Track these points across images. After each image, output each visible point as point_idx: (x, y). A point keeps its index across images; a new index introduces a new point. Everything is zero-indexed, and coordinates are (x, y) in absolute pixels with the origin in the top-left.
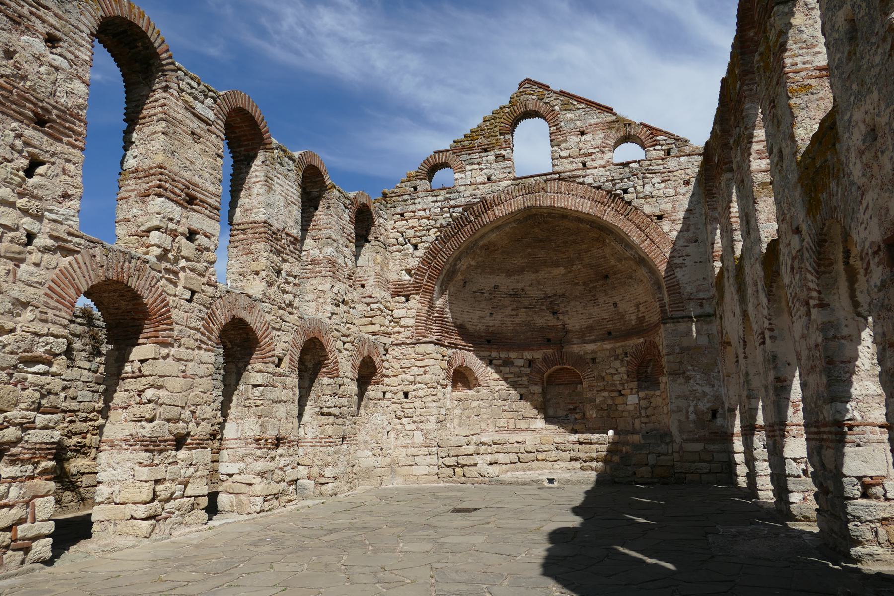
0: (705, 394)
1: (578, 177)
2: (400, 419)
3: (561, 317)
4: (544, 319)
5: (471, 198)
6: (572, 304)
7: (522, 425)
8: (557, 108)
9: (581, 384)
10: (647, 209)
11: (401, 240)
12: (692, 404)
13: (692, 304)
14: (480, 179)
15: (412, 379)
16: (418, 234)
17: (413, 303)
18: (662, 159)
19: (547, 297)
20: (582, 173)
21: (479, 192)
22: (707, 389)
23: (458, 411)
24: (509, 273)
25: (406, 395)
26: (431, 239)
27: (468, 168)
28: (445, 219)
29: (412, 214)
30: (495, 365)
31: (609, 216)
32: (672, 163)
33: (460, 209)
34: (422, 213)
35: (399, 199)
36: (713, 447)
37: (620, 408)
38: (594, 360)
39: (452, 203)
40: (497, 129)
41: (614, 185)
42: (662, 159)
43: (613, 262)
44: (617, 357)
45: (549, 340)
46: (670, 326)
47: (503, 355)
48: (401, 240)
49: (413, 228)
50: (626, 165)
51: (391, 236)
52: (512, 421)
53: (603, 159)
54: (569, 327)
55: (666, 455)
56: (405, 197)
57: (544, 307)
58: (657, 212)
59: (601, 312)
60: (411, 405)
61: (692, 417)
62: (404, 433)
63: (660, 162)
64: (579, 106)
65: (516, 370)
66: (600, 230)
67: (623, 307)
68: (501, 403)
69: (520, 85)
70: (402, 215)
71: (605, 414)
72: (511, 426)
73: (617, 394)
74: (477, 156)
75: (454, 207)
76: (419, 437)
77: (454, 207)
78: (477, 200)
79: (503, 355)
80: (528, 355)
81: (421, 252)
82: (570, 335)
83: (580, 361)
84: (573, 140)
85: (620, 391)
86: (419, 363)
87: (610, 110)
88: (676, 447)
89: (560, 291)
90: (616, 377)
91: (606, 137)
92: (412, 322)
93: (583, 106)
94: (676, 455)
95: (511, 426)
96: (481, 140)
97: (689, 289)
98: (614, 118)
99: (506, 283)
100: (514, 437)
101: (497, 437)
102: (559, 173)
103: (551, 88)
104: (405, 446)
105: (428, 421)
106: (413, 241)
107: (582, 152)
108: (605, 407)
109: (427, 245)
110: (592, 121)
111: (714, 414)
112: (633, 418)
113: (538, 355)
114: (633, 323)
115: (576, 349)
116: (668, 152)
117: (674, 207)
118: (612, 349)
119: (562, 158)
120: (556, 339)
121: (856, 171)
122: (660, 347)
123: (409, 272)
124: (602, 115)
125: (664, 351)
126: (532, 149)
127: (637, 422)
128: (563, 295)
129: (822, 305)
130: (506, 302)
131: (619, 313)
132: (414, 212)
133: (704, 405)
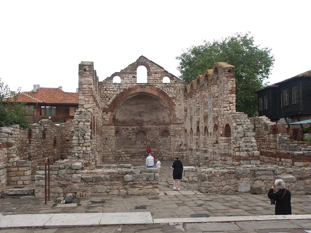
0: (179, 141)
1: (155, 85)
2: (105, 145)
3: (142, 117)
4: (137, 118)
5: (126, 88)
6: (145, 114)
7: (130, 146)
8: (150, 65)
9: (146, 135)
10: (170, 96)
11: (105, 96)
12: (177, 143)
13: (178, 120)
14: (128, 82)
15: (108, 135)
16: (110, 95)
17: (109, 115)
18: (174, 83)
19: (139, 112)
20: (154, 84)
21: (129, 86)
22: (180, 140)
23: (116, 143)
24: (130, 105)
25: (106, 139)
26: (114, 97)
27: (125, 78)
28: (118, 92)
29: (109, 90)
30: (125, 130)
31: (161, 97)
32: (176, 85)
33: (123, 90)
34: (112, 90)
35: (105, 84)
36: (180, 153)
37: (157, 142)
38: (150, 130)
39: (121, 88)
40: (133, 69)
41: (163, 89)
42: (174, 83)
43: (159, 106)
44: (157, 130)
45: (138, 123)
46: (173, 125)
47: (126, 127)
48: (105, 96)
49: (109, 93)
50: (166, 84)
51: (103, 95)
52: (127, 145)
53: (160, 81)
54: (144, 120)
55: (170, 154)
56: (107, 84)
57: (138, 115)
58: (172, 97)
59: (153, 117)
60: (108, 142)
61: (176, 146)
62: (106, 149)
63: (174, 84)
64: (155, 66)
65: (129, 131)
66: (157, 99)
67: (159, 117)
68: (125, 140)
69: (140, 57)
70: (106, 89)
71: (152, 144)
72: (128, 147)
73: (156, 139)
74: (127, 75)
75: (121, 89)
76: (110, 150)
77: (121, 89)
78: (128, 88)
79: (126, 127)
80: (133, 127)
81: (111, 101)
82: (144, 123)
83: (146, 129)
84: (153, 75)
85: (157, 138)
86: (110, 131)
87: (163, 68)
88: (172, 152)
89: (142, 111)
90: (156, 135)
91: (161, 76)
92: (108, 120)
93: (156, 66)
94: (172, 154)
95: (128, 147)
96: (129, 71)
97: (178, 116)
98: (163, 71)
99: (129, 108)
100: (130, 150)
101: (126, 150)
102: (149, 83)
103: (149, 59)
104: (106, 152)
105: (113, 146)
106: (109, 97)
107: (155, 79)
108: (152, 142)
109: (113, 99)
110: (158, 71)
111: (181, 145)
112: (160, 145)
113: (135, 127)
114: (162, 121)
115: (145, 126)
116: (176, 82)
117: (176, 96)
118: (155, 127)
119: (149, 79)
120: (140, 123)
121: (209, 124)
122: (169, 129)
123: (108, 105)
124: (161, 69)
125: (172, 130)
126: (142, 76)
127: (161, 147)
128: (143, 112)
129: (204, 135)
130: (128, 113)
131: (158, 118)
132: (109, 89)
133: (179, 143)
